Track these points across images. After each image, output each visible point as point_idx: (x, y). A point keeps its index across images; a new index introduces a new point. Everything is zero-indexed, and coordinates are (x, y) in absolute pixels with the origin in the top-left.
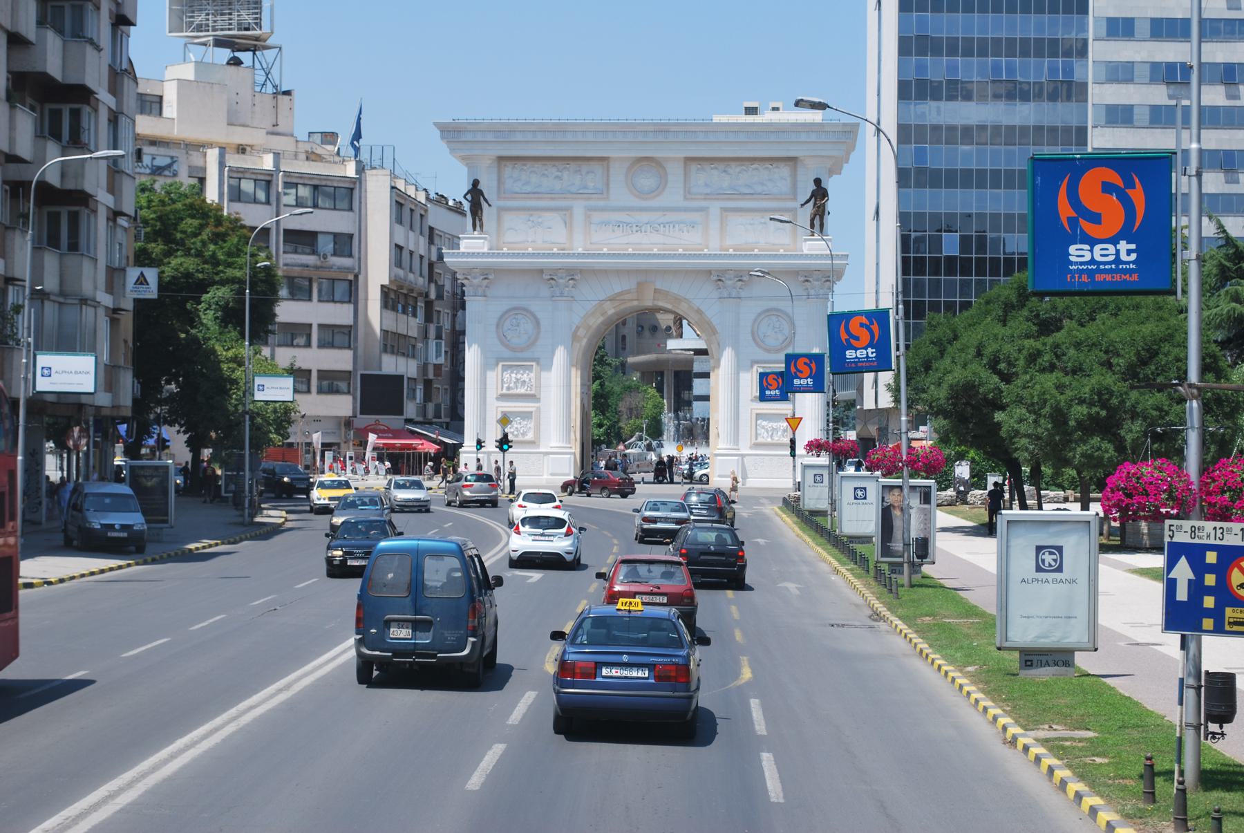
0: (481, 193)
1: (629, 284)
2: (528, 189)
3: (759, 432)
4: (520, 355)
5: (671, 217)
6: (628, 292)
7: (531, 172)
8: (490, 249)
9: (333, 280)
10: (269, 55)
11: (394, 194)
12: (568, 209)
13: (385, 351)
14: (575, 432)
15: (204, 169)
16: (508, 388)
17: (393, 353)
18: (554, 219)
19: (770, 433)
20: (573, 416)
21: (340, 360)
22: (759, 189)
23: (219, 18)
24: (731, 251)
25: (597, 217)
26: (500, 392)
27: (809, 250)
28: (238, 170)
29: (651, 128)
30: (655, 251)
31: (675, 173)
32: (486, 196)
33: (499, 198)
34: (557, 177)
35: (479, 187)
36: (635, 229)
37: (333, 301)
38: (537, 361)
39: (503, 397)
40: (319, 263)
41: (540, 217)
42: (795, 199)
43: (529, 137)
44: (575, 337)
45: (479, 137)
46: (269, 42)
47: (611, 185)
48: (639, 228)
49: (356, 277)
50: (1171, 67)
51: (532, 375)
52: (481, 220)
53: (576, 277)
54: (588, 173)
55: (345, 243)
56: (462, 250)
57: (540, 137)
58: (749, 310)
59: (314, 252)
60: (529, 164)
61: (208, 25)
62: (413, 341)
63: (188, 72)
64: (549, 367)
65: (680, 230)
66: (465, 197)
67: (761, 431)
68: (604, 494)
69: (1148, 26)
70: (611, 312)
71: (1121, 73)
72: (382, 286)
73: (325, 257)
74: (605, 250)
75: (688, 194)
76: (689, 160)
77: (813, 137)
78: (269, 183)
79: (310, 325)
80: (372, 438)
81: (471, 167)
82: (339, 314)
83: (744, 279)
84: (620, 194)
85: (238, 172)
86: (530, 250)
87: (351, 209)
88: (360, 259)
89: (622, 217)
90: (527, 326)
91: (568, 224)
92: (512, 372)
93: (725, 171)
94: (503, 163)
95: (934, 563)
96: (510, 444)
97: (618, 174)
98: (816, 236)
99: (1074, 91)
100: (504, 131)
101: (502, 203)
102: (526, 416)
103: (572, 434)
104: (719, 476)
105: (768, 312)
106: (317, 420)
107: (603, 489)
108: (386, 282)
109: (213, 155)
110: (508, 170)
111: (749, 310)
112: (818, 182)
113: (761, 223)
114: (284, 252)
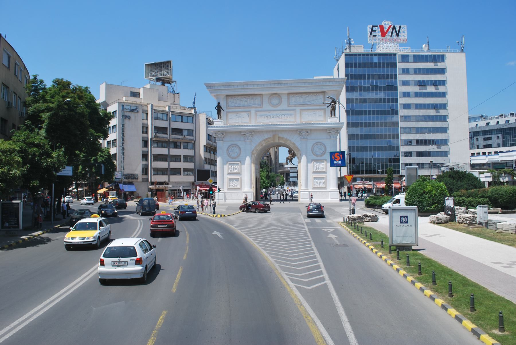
0: (221, 107)
1: (270, 135)
2: (236, 105)
4: (234, 160)
5: (283, 113)
6: (270, 138)
8: (225, 125)
9: (188, 143)
10: (173, 84)
12: (250, 111)
15: (147, 111)
16: (231, 171)
17: (209, 164)
18: (245, 115)
20: (252, 180)
21: (190, 165)
22: (313, 102)
23: (158, 73)
24: (304, 123)
25: (259, 114)
26: (228, 172)
27: (331, 121)
28: (157, 110)
29: (276, 82)
30: (279, 123)
31: (285, 99)
33: (227, 109)
34: (246, 101)
35: (220, 105)
36: (271, 117)
37: (188, 149)
38: (240, 161)
39: (229, 174)
40: (183, 138)
41: (240, 114)
43: (236, 87)
44: (252, 153)
45: (219, 88)
46: (173, 80)
47: (263, 103)
48: (273, 117)
49: (195, 142)
50: (420, 81)
51: (239, 166)
52: (221, 115)
53: (252, 133)
54: (255, 99)
55: (191, 132)
56: (214, 125)
57: (239, 87)
58: (311, 143)
59: (182, 135)
60: (236, 97)
61: (155, 75)
63: (148, 86)
64: (244, 163)
69: (413, 71)
70: (264, 145)
71: (405, 83)
72: (204, 145)
73: (185, 136)
74: (262, 124)
75: (289, 105)
76: (289, 94)
77: (331, 84)
78: (167, 114)
79: (181, 156)
80: (198, 188)
81: (217, 99)
82: (189, 152)
84: (266, 106)
85: (157, 111)
86: (237, 125)
87: (193, 123)
88: (195, 137)
89: (268, 113)
90: (237, 150)
91: (250, 116)
92: (232, 166)
93: (301, 97)
94: (228, 97)
95: (418, 245)
97: (265, 100)
98: (333, 116)
99: (394, 88)
100: (227, 86)
102: (237, 180)
103: (252, 185)
104: (302, 199)
105: (317, 143)
106: (184, 183)
108: (205, 144)
109: (150, 106)
110: (230, 99)
111: (311, 143)
113: (314, 114)
114: (172, 134)
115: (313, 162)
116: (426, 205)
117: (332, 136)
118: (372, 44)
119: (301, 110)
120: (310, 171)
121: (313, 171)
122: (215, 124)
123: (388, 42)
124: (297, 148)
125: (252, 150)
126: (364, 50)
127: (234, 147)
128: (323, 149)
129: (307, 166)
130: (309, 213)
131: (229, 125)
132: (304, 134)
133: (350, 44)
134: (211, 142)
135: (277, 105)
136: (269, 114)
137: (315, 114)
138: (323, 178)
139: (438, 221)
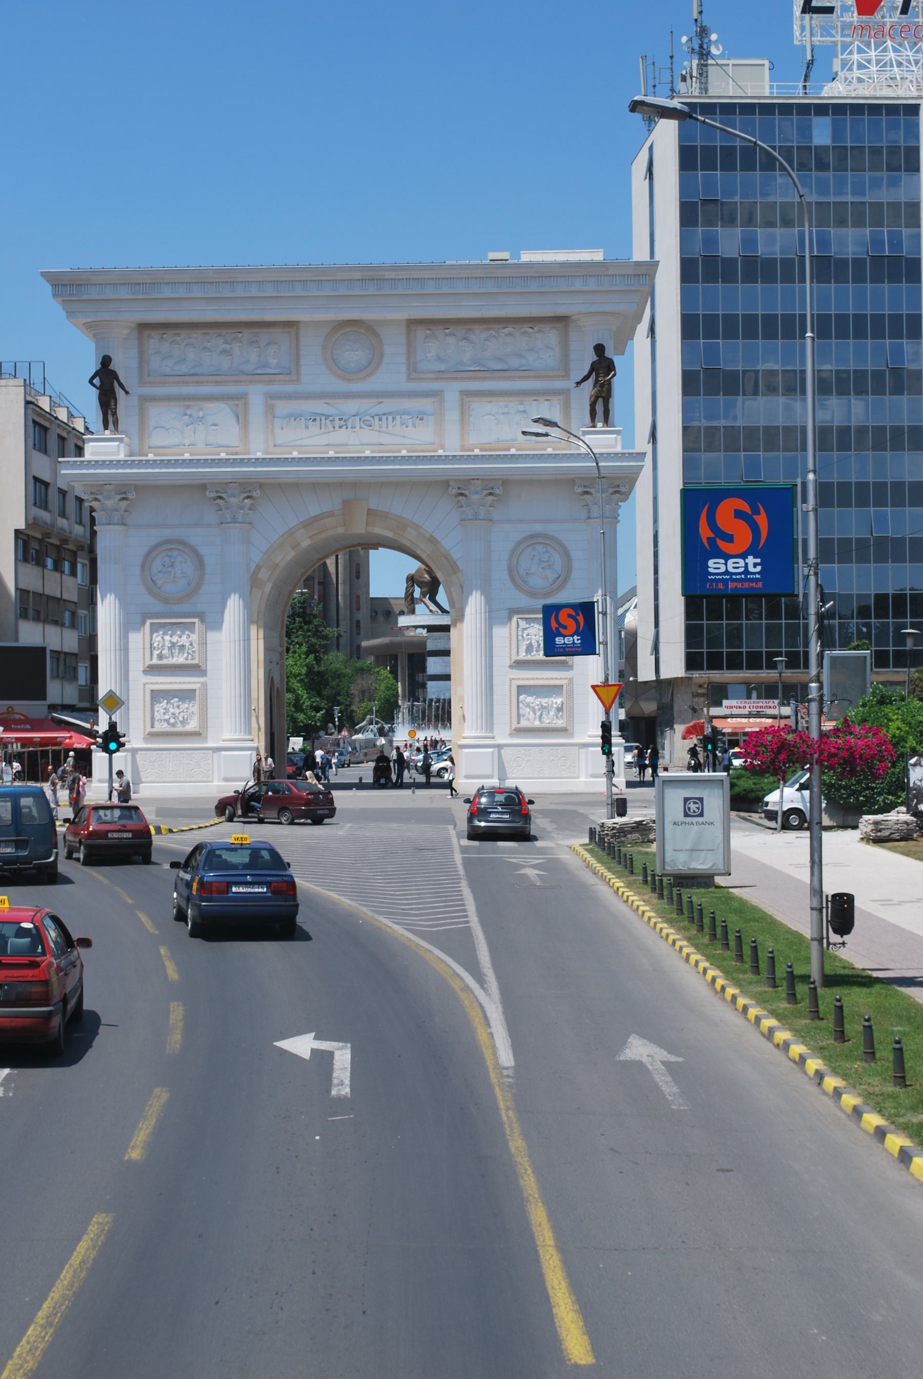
0: (114, 376)
1: (331, 503)
2: (183, 369)
3: (521, 712)
4: (175, 608)
5: (389, 405)
6: (330, 514)
7: (186, 345)
11: (30, 411)
13: (24, 614)
14: (257, 718)
16: (160, 657)
17: (37, 619)
18: (221, 412)
19: (538, 714)
20: (254, 695)
22: (515, 363)
24: (477, 452)
25: (283, 407)
26: (148, 662)
29: (358, 275)
30: (368, 453)
32: (122, 380)
33: (142, 383)
35: (111, 367)
38: (201, 616)
39: (152, 670)
41: (201, 409)
42: (566, 376)
44: (255, 582)
45: (109, 294)
47: (302, 362)
48: (344, 421)
51: (194, 637)
52: (114, 414)
53: (254, 494)
54: (269, 344)
56: (88, 455)
57: (197, 292)
60: (184, 333)
62: (72, 606)
64: (217, 625)
65: (402, 424)
66: (91, 381)
67: (525, 711)
68: (283, 819)
70: (306, 543)
72: (17, 532)
74: (295, 454)
75: (413, 372)
76: (413, 324)
77: (592, 285)
81: (99, 340)
83: (497, 491)
86: (187, 456)
89: (319, 406)
90: (185, 567)
91: (242, 419)
93: (465, 338)
96: (122, 740)
98: (600, 425)
101: (147, 391)
102: (187, 695)
103: (254, 720)
104: (467, 777)
105: (533, 539)
107: (282, 810)
108: (22, 526)
110: (154, 343)
112: (599, 349)
113: (519, 411)
115: (514, 619)
116: (882, 789)
117: (595, 511)
118: (809, 57)
119: (466, 394)
120: (502, 659)
121: (514, 658)
122: (92, 450)
123: (889, 43)
124: (447, 557)
125: (252, 569)
126: (771, 87)
127: (175, 553)
128: (558, 564)
129: (489, 637)
130: (477, 823)
131: (151, 456)
132: (475, 498)
133: (703, 54)
134: (45, 516)
135: (361, 370)
136: (327, 410)
137: (524, 412)
138: (555, 690)
139: (879, 834)
